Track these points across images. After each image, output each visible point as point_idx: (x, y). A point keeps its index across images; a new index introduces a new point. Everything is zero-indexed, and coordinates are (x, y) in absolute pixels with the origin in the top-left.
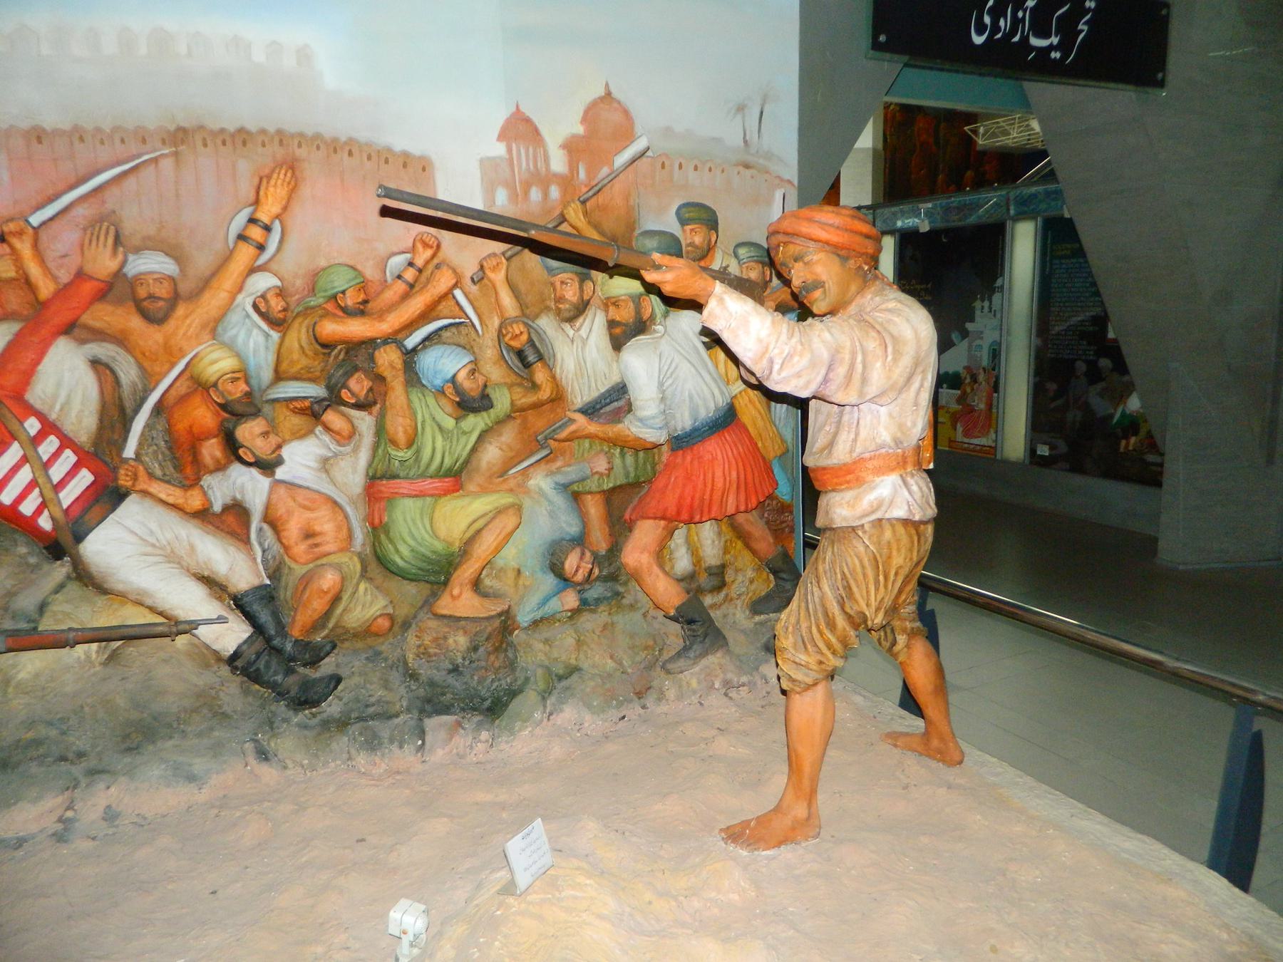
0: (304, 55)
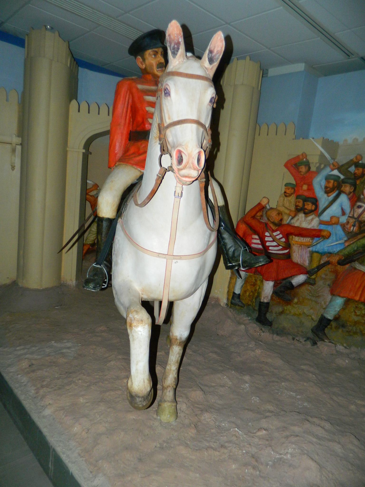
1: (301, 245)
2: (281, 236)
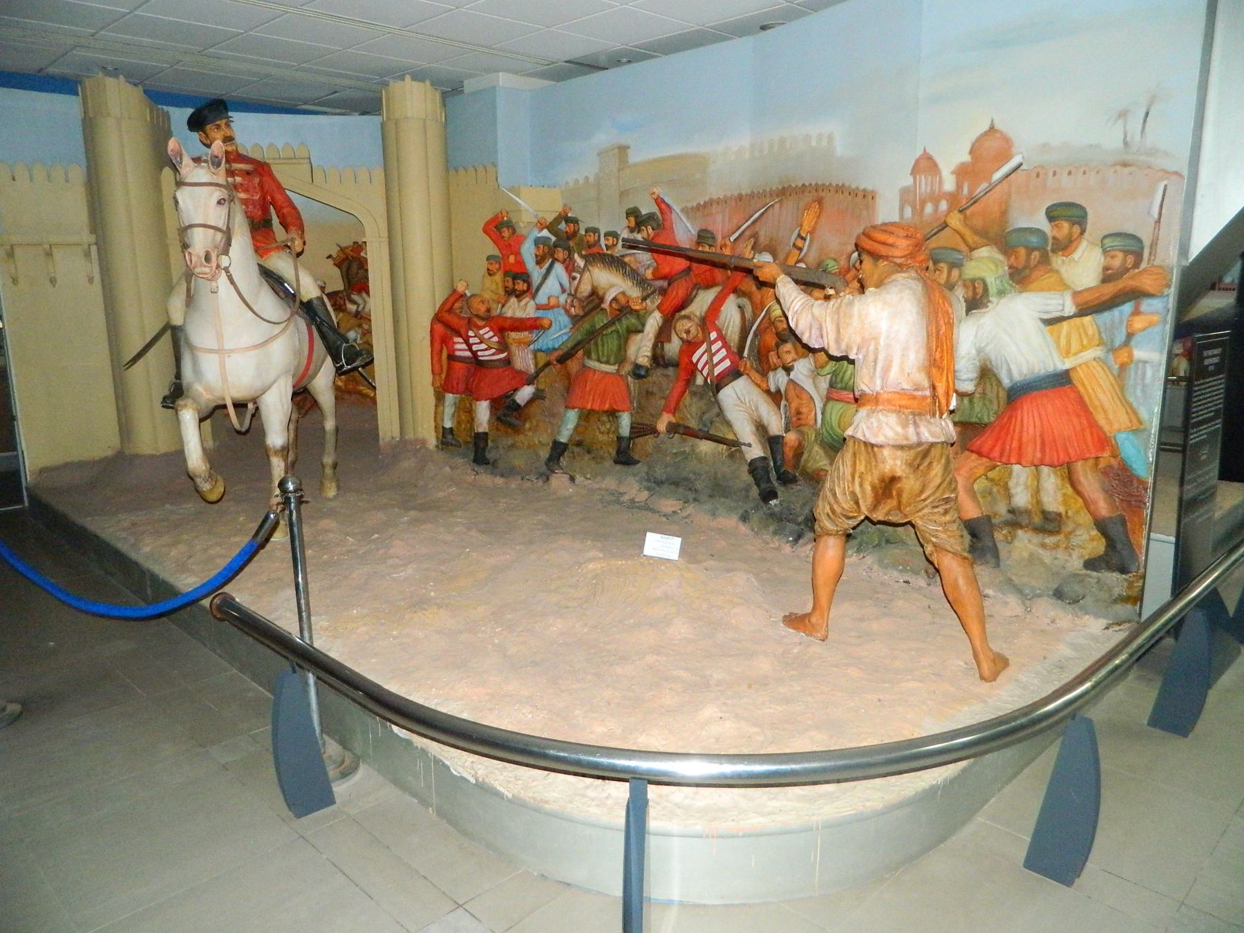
0: (831, 138)
1: (520, 342)
2: (491, 334)
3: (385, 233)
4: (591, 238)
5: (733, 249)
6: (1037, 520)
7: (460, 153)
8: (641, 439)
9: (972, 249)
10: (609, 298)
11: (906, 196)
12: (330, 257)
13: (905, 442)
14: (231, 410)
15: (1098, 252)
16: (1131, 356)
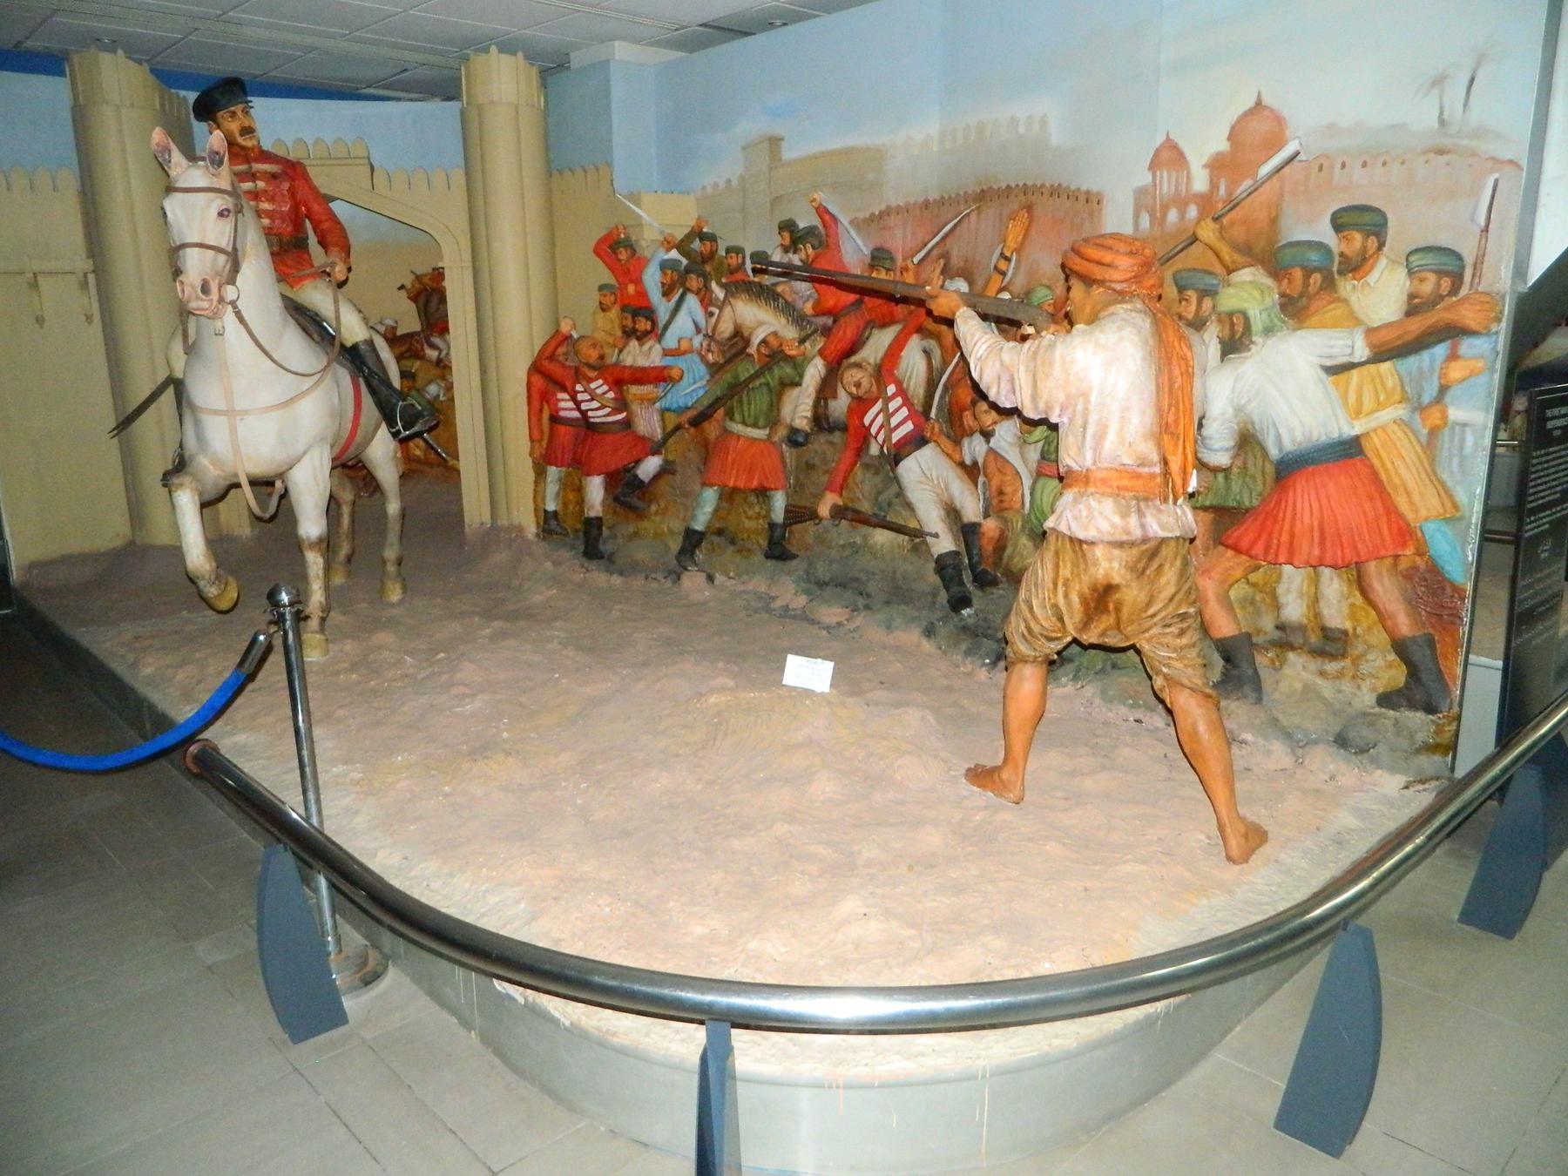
0: (1044, 122)
1: (642, 399)
2: (605, 388)
3: (468, 257)
4: (734, 260)
5: (917, 274)
6: (1314, 639)
7: (566, 152)
8: (799, 527)
9: (1230, 272)
10: (756, 340)
11: (1144, 199)
12: (402, 287)
13: (1125, 538)
14: (247, 488)
15: (1401, 274)
16: (1444, 416)
